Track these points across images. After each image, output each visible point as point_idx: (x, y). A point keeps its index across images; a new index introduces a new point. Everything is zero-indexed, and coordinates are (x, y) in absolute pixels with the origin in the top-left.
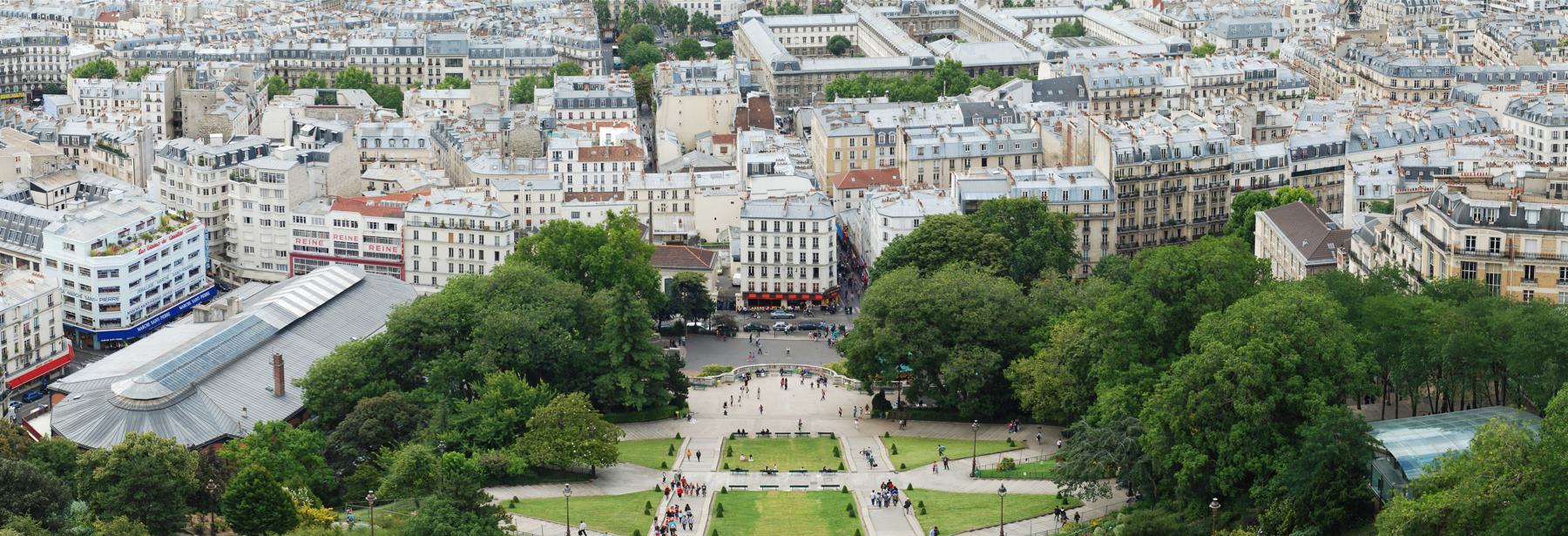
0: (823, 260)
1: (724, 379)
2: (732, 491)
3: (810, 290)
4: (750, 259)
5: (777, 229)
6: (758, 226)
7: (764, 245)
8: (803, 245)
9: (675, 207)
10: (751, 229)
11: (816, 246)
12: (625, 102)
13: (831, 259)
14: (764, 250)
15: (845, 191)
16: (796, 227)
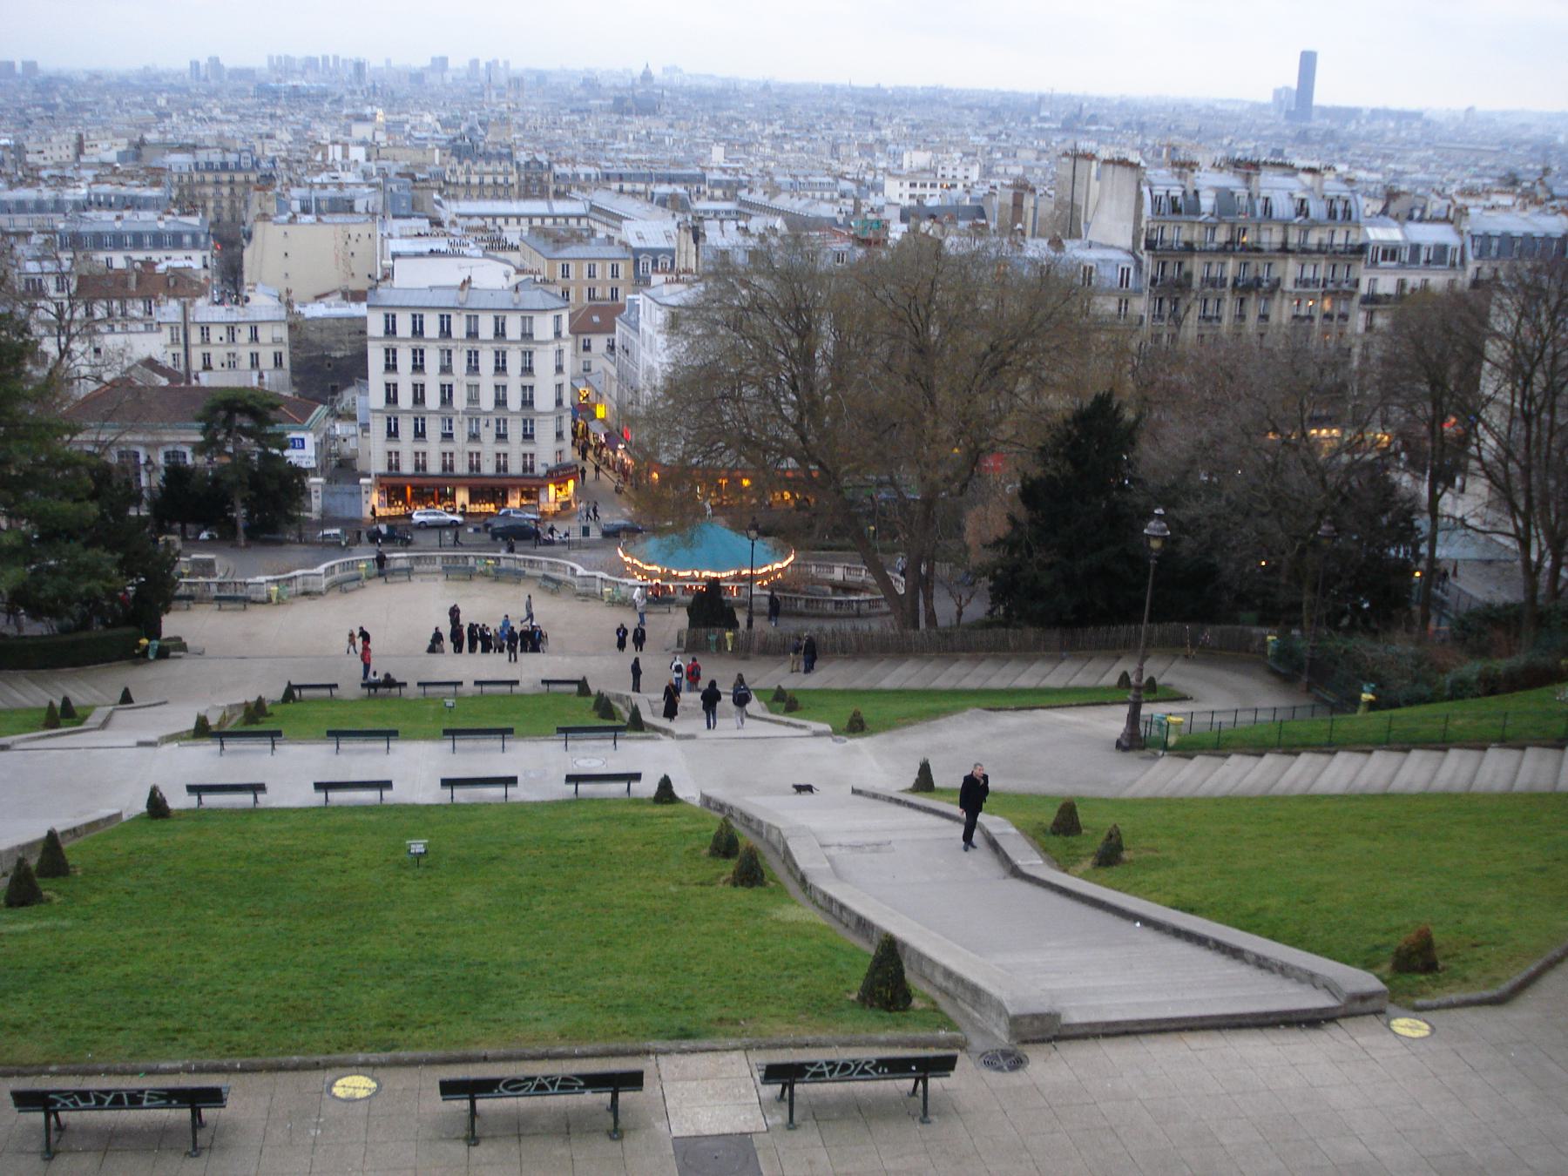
0: (544, 400)
1: (298, 586)
2: (199, 816)
3: (515, 468)
4: (388, 400)
5: (446, 333)
6: (404, 326)
7: (418, 367)
8: (501, 368)
9: (255, 360)
10: (390, 331)
11: (528, 370)
12: (187, 239)
13: (559, 402)
14: (418, 378)
15: (581, 338)
16: (486, 328)
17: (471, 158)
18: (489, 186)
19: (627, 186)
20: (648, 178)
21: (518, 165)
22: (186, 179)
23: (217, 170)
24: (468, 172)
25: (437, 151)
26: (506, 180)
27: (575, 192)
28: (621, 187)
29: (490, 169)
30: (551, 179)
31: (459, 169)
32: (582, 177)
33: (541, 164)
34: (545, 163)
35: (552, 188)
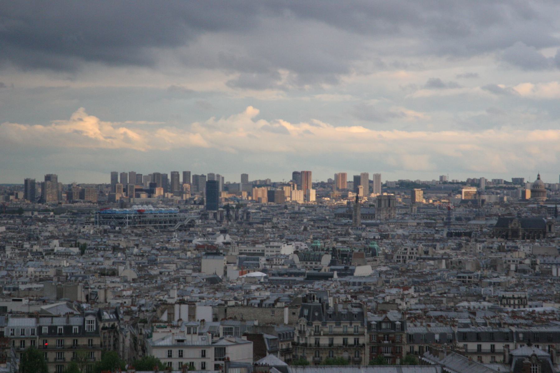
17: (320, 319)
18: (339, 347)
19: (486, 346)
20: (507, 337)
21: (369, 325)
22: (28, 344)
23: (60, 334)
24: (317, 333)
25: (287, 310)
26: (356, 341)
27: (428, 357)
28: (479, 347)
29: (340, 330)
30: (404, 340)
31: (309, 330)
32: (437, 337)
33: (393, 324)
34: (398, 323)
35: (406, 349)
